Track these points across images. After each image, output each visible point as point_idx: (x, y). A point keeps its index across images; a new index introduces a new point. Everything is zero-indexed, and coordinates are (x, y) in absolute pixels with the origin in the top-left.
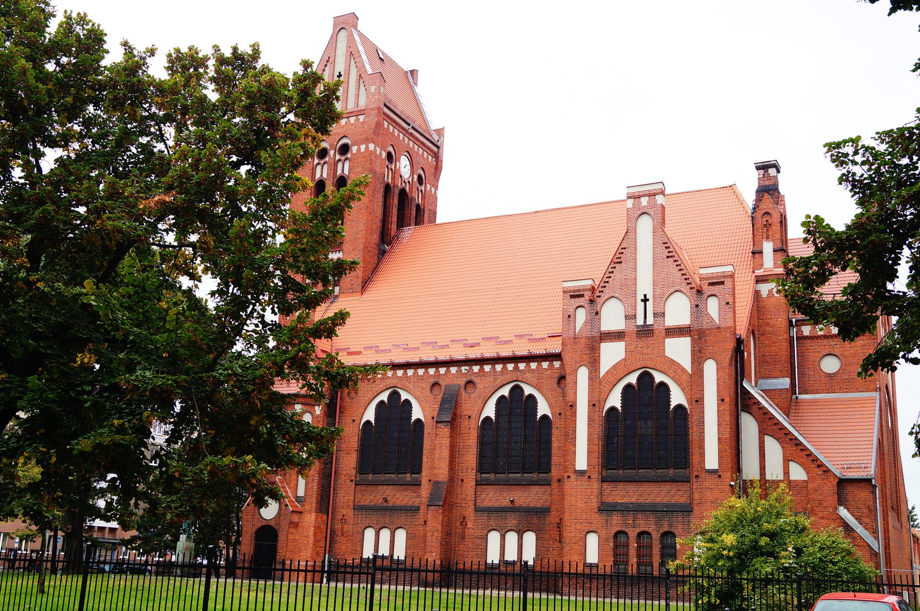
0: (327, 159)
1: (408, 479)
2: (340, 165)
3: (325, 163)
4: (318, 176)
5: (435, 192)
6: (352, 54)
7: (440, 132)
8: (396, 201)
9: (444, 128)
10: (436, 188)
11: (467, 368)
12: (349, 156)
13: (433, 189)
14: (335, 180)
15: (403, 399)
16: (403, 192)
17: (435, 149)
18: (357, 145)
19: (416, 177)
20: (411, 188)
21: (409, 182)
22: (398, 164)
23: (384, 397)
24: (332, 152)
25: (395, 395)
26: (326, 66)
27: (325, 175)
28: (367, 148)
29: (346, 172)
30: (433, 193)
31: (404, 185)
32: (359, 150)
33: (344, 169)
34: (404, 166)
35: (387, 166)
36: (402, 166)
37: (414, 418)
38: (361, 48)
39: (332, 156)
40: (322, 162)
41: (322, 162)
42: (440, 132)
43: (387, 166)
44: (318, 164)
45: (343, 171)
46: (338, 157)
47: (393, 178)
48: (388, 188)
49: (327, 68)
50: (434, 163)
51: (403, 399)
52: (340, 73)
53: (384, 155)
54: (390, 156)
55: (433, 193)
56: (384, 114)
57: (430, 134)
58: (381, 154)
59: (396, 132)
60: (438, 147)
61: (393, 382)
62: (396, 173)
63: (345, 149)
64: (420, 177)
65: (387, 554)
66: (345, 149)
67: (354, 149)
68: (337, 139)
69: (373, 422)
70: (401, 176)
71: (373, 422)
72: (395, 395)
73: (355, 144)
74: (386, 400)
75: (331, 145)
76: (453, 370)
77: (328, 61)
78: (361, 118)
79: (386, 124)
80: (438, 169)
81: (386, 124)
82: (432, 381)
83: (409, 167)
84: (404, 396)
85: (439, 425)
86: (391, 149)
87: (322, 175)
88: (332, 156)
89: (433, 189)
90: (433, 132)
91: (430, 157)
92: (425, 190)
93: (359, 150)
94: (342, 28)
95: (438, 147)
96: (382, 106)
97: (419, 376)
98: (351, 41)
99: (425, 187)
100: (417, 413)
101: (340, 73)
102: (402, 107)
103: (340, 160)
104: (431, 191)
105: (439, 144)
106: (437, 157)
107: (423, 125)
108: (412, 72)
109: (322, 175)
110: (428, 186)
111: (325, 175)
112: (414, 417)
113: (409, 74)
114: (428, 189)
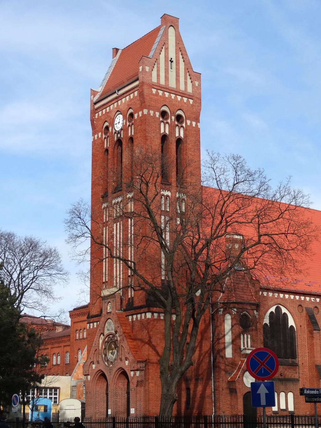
1: (291, 362)
11: (314, 299)
15: (283, 312)
23: (273, 309)
25: (278, 309)
29: (182, 135)
37: (290, 325)
40: (165, 121)
45: (179, 134)
49: (163, 50)
51: (283, 312)
61: (279, 301)
63: (179, 118)
65: (285, 408)
68: (177, 109)
69: (269, 325)
71: (269, 325)
72: (278, 309)
73: (189, 119)
74: (274, 311)
76: (308, 299)
82: (298, 303)
84: (284, 310)
85: (315, 332)
87: (165, 131)
93: (191, 124)
97: (291, 300)
100: (291, 322)
101: (171, 59)
109: (165, 131)
112: (290, 325)
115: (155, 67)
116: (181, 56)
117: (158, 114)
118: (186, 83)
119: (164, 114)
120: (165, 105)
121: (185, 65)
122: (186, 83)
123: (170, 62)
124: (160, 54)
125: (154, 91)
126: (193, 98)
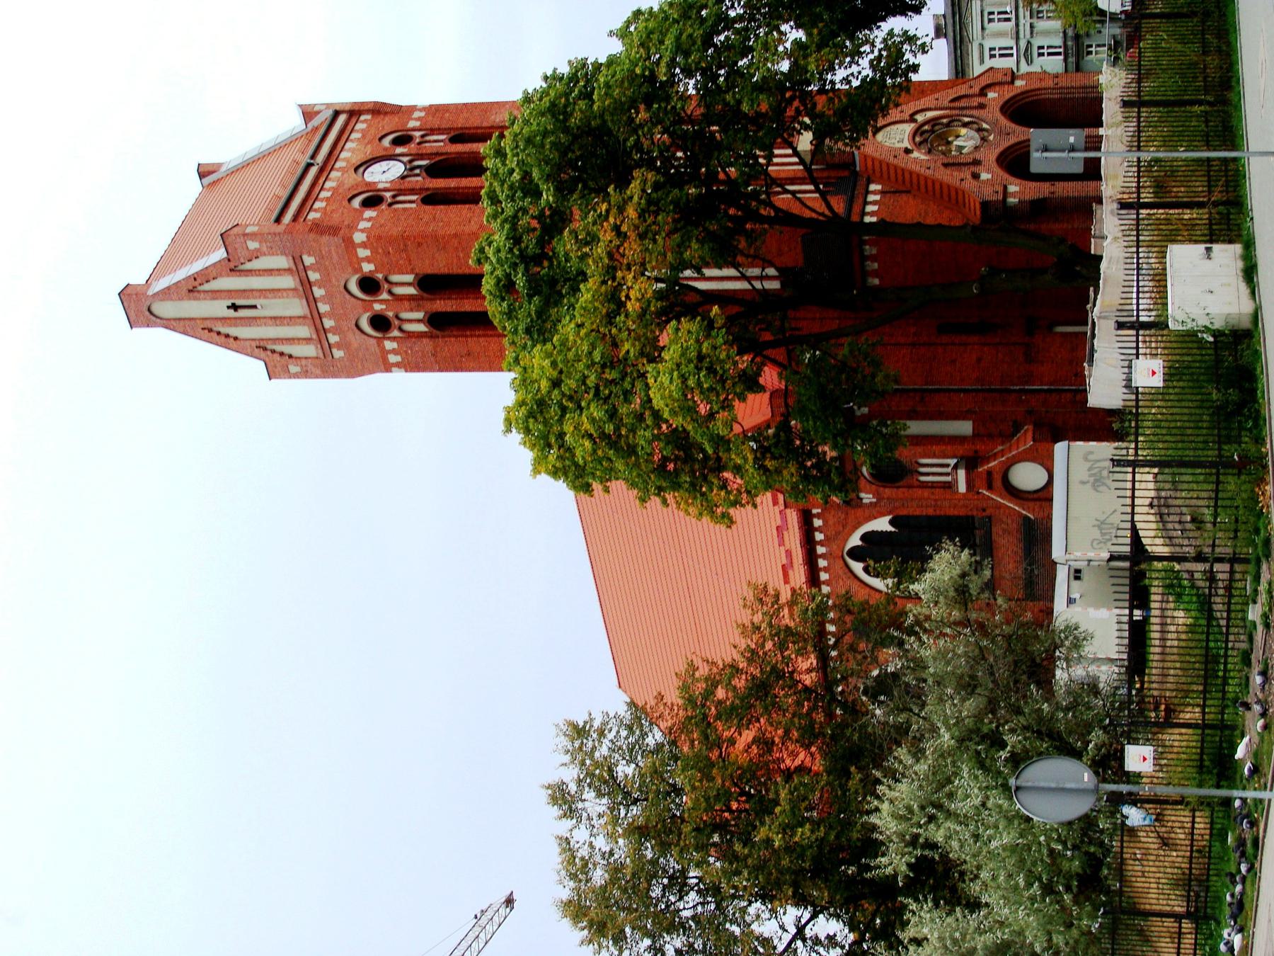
0: (390, 314)
2: (399, 291)
3: (397, 317)
4: (422, 328)
5: (424, 109)
6: (193, 288)
7: (308, 114)
8: (452, 183)
9: (300, 106)
10: (412, 109)
12: (380, 276)
13: (417, 114)
14: (425, 295)
16: (433, 171)
17: (342, 119)
18: (359, 264)
19: (399, 150)
20: (421, 156)
21: (410, 162)
22: (381, 186)
24: (377, 307)
26: (219, 333)
27: (420, 315)
28: (364, 245)
29: (409, 278)
30: (423, 114)
31: (417, 171)
32: (368, 260)
33: (404, 284)
34: (385, 174)
35: (390, 205)
36: (384, 178)
38: (181, 274)
39: (384, 307)
41: (397, 322)
42: (308, 114)
43: (390, 205)
44: (400, 329)
45: (409, 284)
46: (385, 296)
47: (412, 191)
48: (432, 199)
49: (224, 330)
50: (368, 117)
52: (228, 307)
53: (369, 213)
54: (373, 201)
55: (423, 114)
56: (295, 218)
57: (317, 129)
58: (369, 219)
59: (324, 194)
60: (337, 114)
62: (400, 189)
63: (369, 285)
64: (398, 142)
66: (369, 285)
67: (367, 268)
70: (403, 177)
75: (366, 310)
77: (210, 330)
78: (309, 260)
79: (312, 216)
80: (378, 110)
81: (312, 216)
83: (384, 165)
86: (356, 202)
87: (419, 321)
88: (384, 307)
89: (417, 114)
90: (310, 126)
91: (360, 126)
92: (419, 130)
94: (149, 310)
95: (337, 114)
96: (281, 228)
98: (166, 294)
99: (414, 129)
101: (228, 307)
102: (273, 185)
103: (390, 292)
104: (418, 119)
105: (329, 113)
106: (354, 112)
107: (299, 144)
108: (203, 172)
109: (419, 321)
110: (412, 124)
111: (420, 315)
113: (207, 180)
114: (417, 124)
115: (279, 348)
116: (206, 287)
117: (389, 345)
118: (269, 272)
119: (380, 323)
120: (357, 326)
121: (221, 276)
122: (269, 272)
123: (242, 313)
124: (236, 338)
125: (338, 354)
126: (297, 256)
